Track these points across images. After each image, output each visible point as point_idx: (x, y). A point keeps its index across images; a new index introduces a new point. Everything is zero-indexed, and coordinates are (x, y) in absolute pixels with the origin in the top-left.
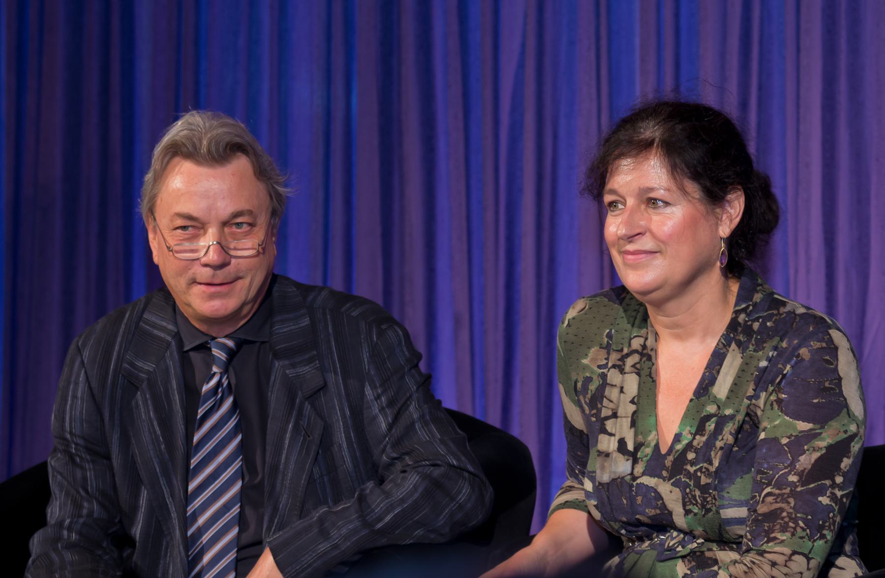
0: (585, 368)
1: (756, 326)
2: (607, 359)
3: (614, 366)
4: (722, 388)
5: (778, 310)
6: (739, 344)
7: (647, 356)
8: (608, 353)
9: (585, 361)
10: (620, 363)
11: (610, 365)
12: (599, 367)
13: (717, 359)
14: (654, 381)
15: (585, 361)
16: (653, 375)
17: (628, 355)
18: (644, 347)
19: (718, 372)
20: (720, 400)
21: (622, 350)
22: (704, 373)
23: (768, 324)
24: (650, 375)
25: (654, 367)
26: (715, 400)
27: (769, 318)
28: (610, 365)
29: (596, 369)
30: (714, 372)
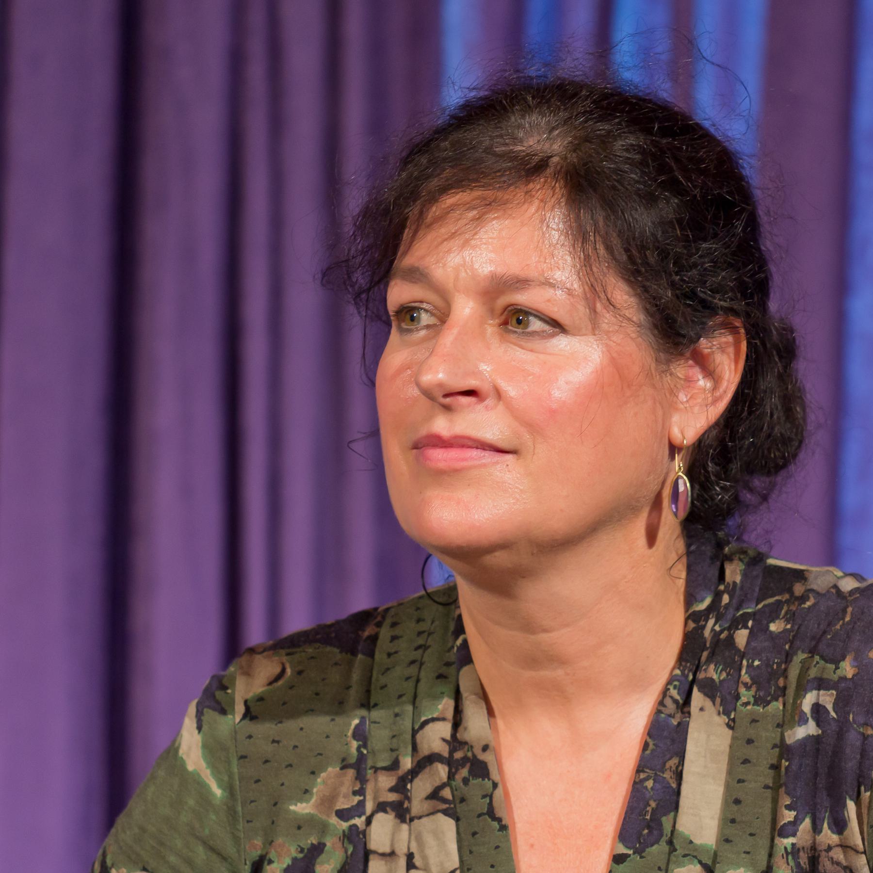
0: (300, 824)
1: (741, 637)
2: (361, 792)
3: (382, 807)
4: (701, 813)
5: (790, 591)
6: (710, 689)
7: (471, 766)
8: (361, 778)
9: (302, 808)
10: (393, 797)
11: (369, 807)
12: (342, 815)
13: (665, 742)
14: (503, 828)
15: (302, 808)
16: (499, 813)
17: (414, 773)
18: (455, 742)
19: (679, 776)
20: (703, 849)
21: (394, 765)
22: (637, 787)
23: (773, 627)
24: (491, 813)
25: (498, 793)
26: (692, 852)
27: (773, 613)
28: (369, 807)
29: (334, 820)
30: (667, 775)
